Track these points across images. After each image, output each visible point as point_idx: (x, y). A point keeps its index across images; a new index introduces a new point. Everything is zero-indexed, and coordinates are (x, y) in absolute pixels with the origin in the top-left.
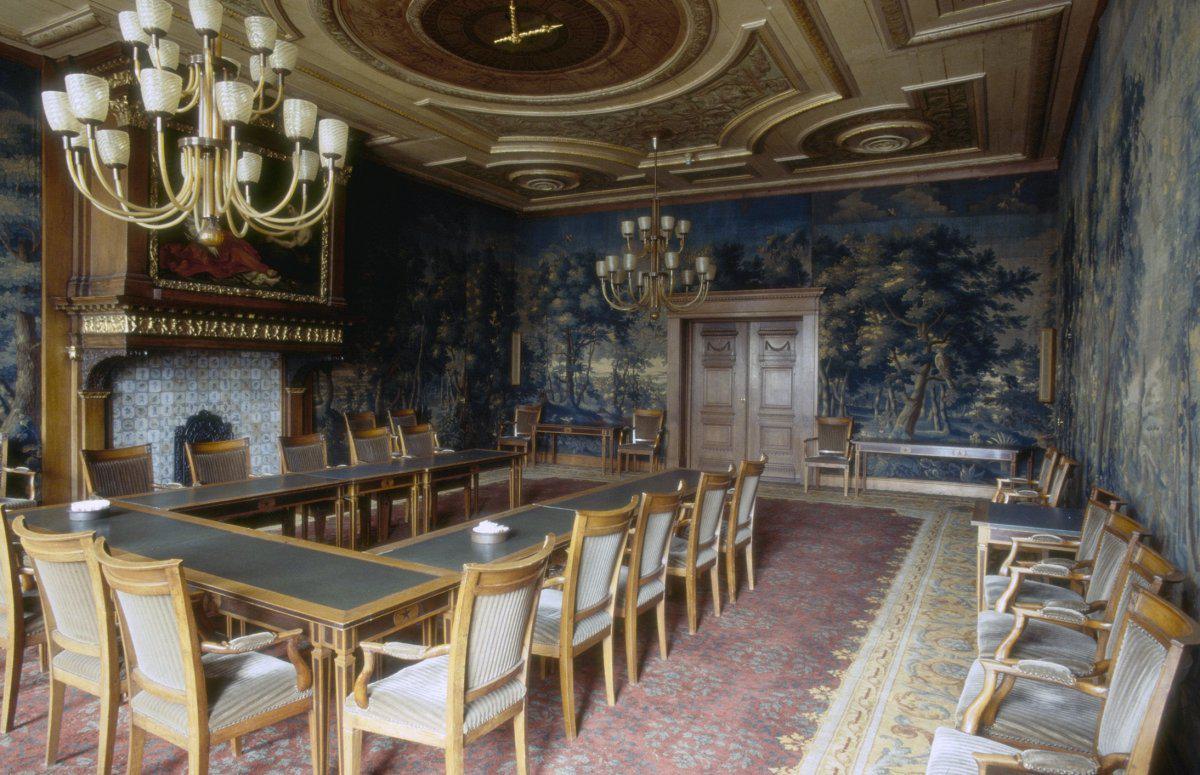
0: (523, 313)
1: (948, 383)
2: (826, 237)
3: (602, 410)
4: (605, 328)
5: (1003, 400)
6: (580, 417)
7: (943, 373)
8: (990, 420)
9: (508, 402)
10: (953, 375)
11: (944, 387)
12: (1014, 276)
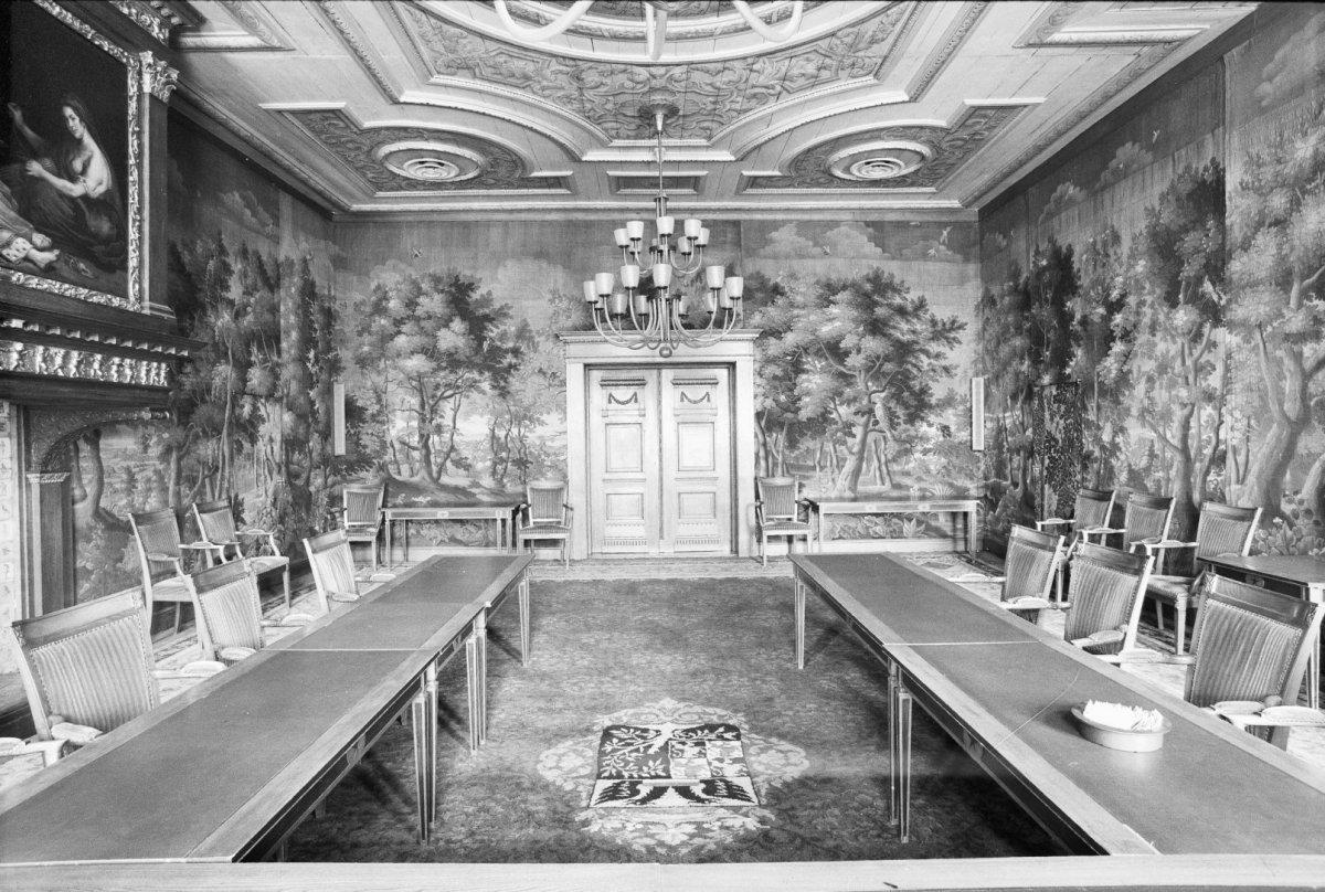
0: (346, 355)
1: (888, 435)
2: (758, 273)
3: (476, 485)
4: (475, 375)
5: (938, 450)
6: (442, 497)
7: (883, 424)
8: (928, 471)
9: (330, 480)
10: (893, 426)
11: (885, 438)
12: (944, 324)
